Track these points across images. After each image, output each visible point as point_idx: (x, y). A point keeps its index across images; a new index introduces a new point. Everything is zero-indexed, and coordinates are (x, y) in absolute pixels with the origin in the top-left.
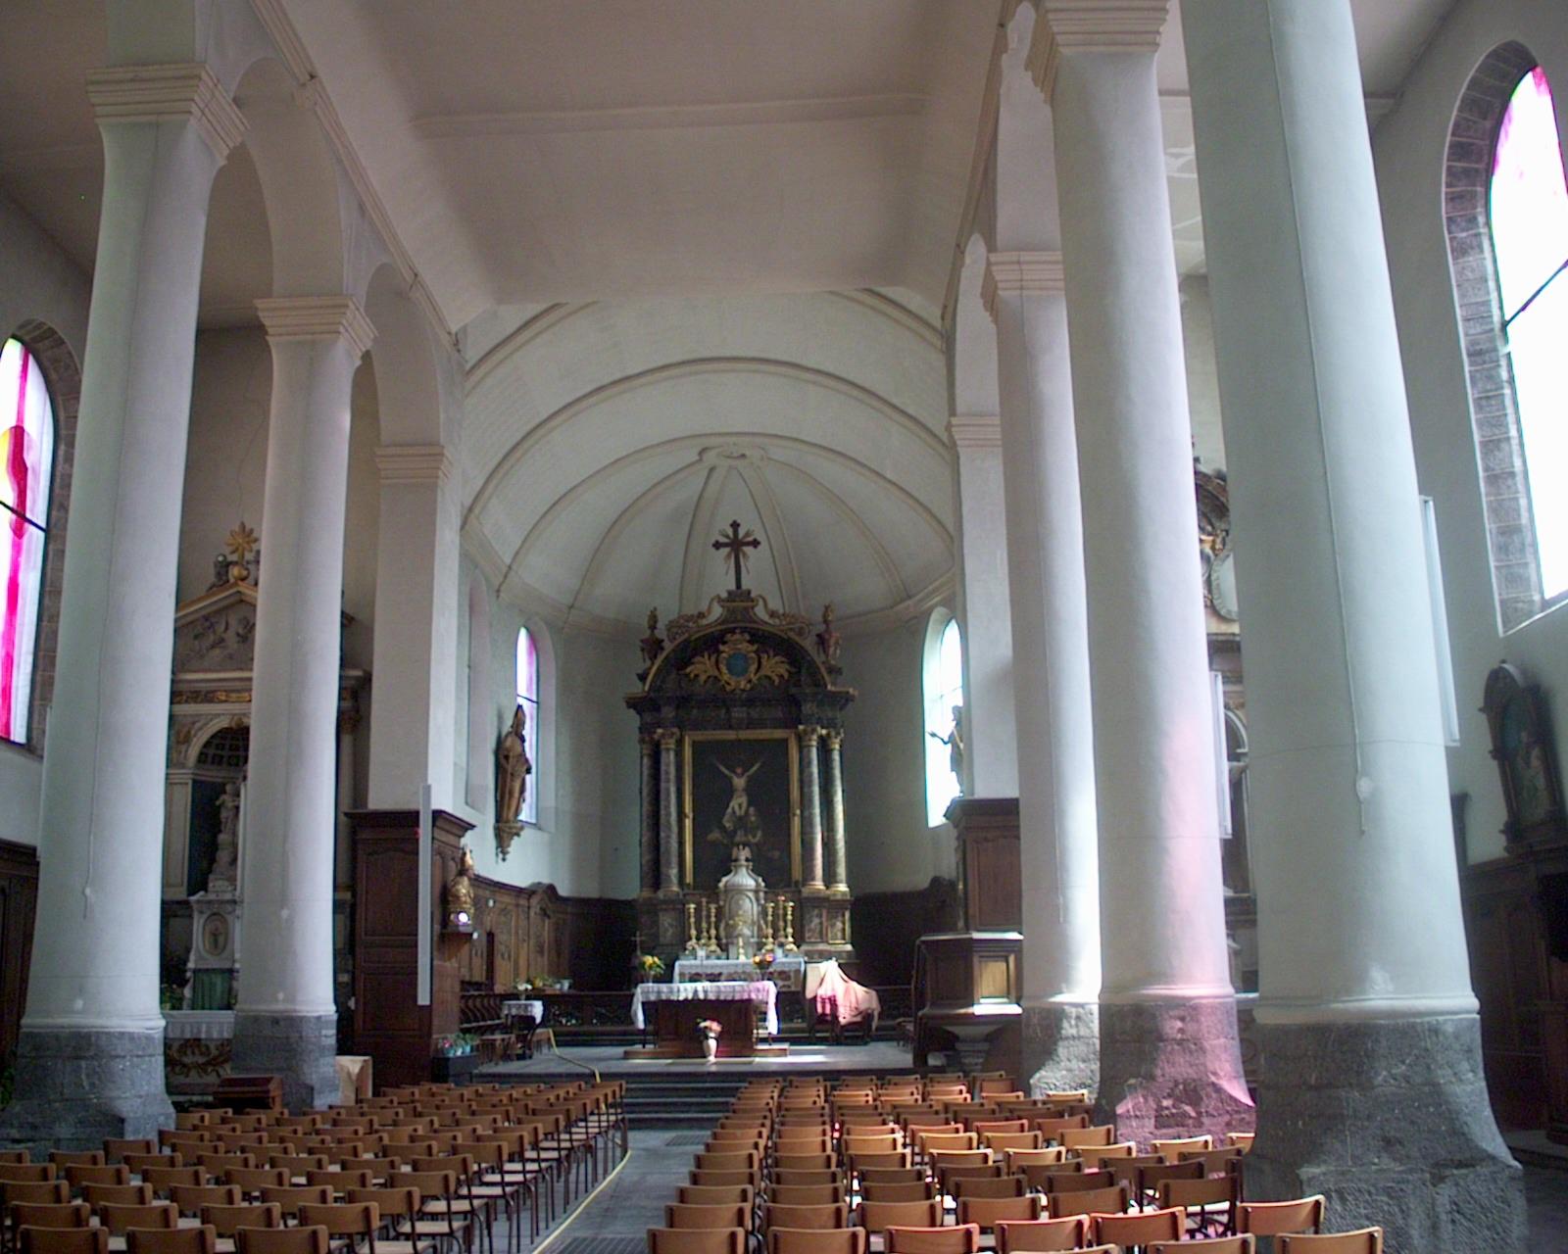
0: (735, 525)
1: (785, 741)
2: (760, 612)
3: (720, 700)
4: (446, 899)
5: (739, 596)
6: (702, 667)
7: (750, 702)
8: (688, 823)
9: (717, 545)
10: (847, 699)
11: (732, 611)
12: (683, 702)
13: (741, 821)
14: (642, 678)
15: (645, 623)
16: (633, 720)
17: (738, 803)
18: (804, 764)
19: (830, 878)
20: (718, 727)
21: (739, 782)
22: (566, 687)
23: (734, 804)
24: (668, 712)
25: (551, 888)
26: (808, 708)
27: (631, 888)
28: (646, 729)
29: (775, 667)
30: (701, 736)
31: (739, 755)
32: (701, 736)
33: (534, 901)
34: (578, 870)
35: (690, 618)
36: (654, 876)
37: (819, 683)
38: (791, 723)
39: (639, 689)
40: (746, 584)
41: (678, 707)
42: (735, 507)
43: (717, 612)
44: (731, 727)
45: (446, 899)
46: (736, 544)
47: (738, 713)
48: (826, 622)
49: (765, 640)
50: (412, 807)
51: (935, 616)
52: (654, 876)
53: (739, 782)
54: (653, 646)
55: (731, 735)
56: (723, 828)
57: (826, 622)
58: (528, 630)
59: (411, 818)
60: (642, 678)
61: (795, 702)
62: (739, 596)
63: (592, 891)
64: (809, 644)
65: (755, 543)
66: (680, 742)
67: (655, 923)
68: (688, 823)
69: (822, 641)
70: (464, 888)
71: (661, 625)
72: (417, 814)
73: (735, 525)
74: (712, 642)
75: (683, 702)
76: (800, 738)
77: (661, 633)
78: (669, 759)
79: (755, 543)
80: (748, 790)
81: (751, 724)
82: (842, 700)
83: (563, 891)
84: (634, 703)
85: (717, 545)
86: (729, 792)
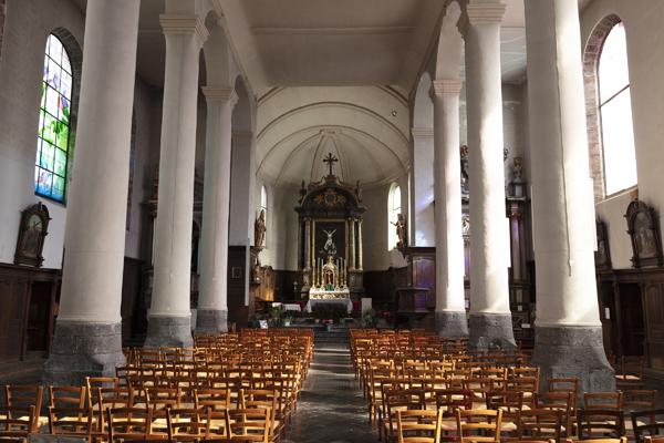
1: (343, 223)
2: (338, 182)
3: (325, 209)
4: (253, 273)
5: (331, 178)
6: (319, 199)
10: (363, 210)
13: (330, 248)
14: (300, 202)
15: (300, 184)
16: (297, 215)
17: (329, 242)
18: (350, 230)
20: (323, 217)
22: (275, 205)
24: (308, 213)
26: (352, 213)
27: (295, 267)
28: (301, 218)
29: (342, 199)
31: (329, 227)
34: (278, 262)
36: (302, 264)
37: (355, 205)
39: (298, 205)
42: (330, 149)
43: (324, 182)
44: (327, 217)
45: (253, 273)
46: (330, 160)
47: (329, 214)
49: (340, 191)
50: (243, 245)
51: (393, 184)
52: (302, 264)
54: (303, 192)
55: (327, 221)
59: (244, 248)
60: (300, 202)
61: (347, 211)
62: (331, 178)
63: (282, 268)
64: (352, 192)
69: (357, 192)
70: (258, 270)
71: (306, 185)
72: (244, 248)
74: (322, 191)
77: (306, 187)
78: (308, 228)
80: (332, 238)
82: (362, 210)
83: (274, 268)
84: (297, 209)
86: (327, 238)
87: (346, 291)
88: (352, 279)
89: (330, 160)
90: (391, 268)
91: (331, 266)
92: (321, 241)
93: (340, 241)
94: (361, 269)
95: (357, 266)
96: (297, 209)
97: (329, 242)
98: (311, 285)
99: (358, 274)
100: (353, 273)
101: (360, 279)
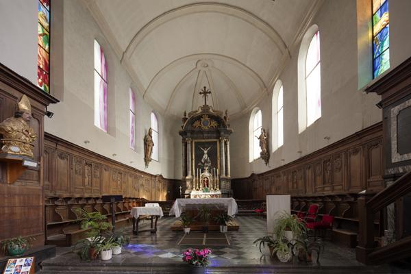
0: (205, 88)
3: (201, 132)
5: (205, 108)
6: (197, 124)
7: (208, 132)
8: (194, 161)
9: (201, 93)
11: (204, 110)
12: (192, 132)
13: (206, 161)
14: (182, 127)
15: (183, 114)
17: (205, 156)
18: (221, 147)
19: (226, 174)
20: (201, 139)
21: (206, 152)
22: (165, 130)
23: (204, 157)
24: (189, 134)
25: (161, 176)
26: (222, 133)
27: (180, 177)
28: (184, 139)
29: (214, 124)
30: (196, 141)
31: (204, 145)
32: (196, 141)
33: (157, 178)
34: (169, 172)
35: (195, 112)
36: (186, 174)
37: (225, 127)
38: (218, 137)
40: (207, 104)
41: (192, 134)
43: (200, 111)
44: (203, 139)
46: (205, 93)
47: (205, 135)
48: (226, 114)
49: (212, 117)
53: (206, 152)
54: (185, 119)
55: (203, 141)
56: (202, 163)
57: (226, 114)
58: (155, 114)
62: (205, 108)
63: (172, 178)
64: (223, 117)
65: (210, 93)
66: (192, 142)
67: (186, 184)
68: (194, 161)
71: (187, 113)
73: (205, 88)
74: (199, 118)
75: (192, 132)
76: (220, 141)
77: (187, 116)
79: (210, 93)
80: (208, 153)
81: (208, 138)
82: (230, 132)
83: (165, 176)
85: (201, 93)
86: (203, 154)
87: (219, 192)
88: (223, 183)
89: (205, 93)
90: (253, 175)
91: (206, 174)
92: (199, 157)
93: (213, 155)
94: (229, 176)
95: (226, 174)
96: (181, 133)
97: (205, 156)
98: (192, 188)
99: (227, 180)
100: (224, 179)
101: (229, 184)
